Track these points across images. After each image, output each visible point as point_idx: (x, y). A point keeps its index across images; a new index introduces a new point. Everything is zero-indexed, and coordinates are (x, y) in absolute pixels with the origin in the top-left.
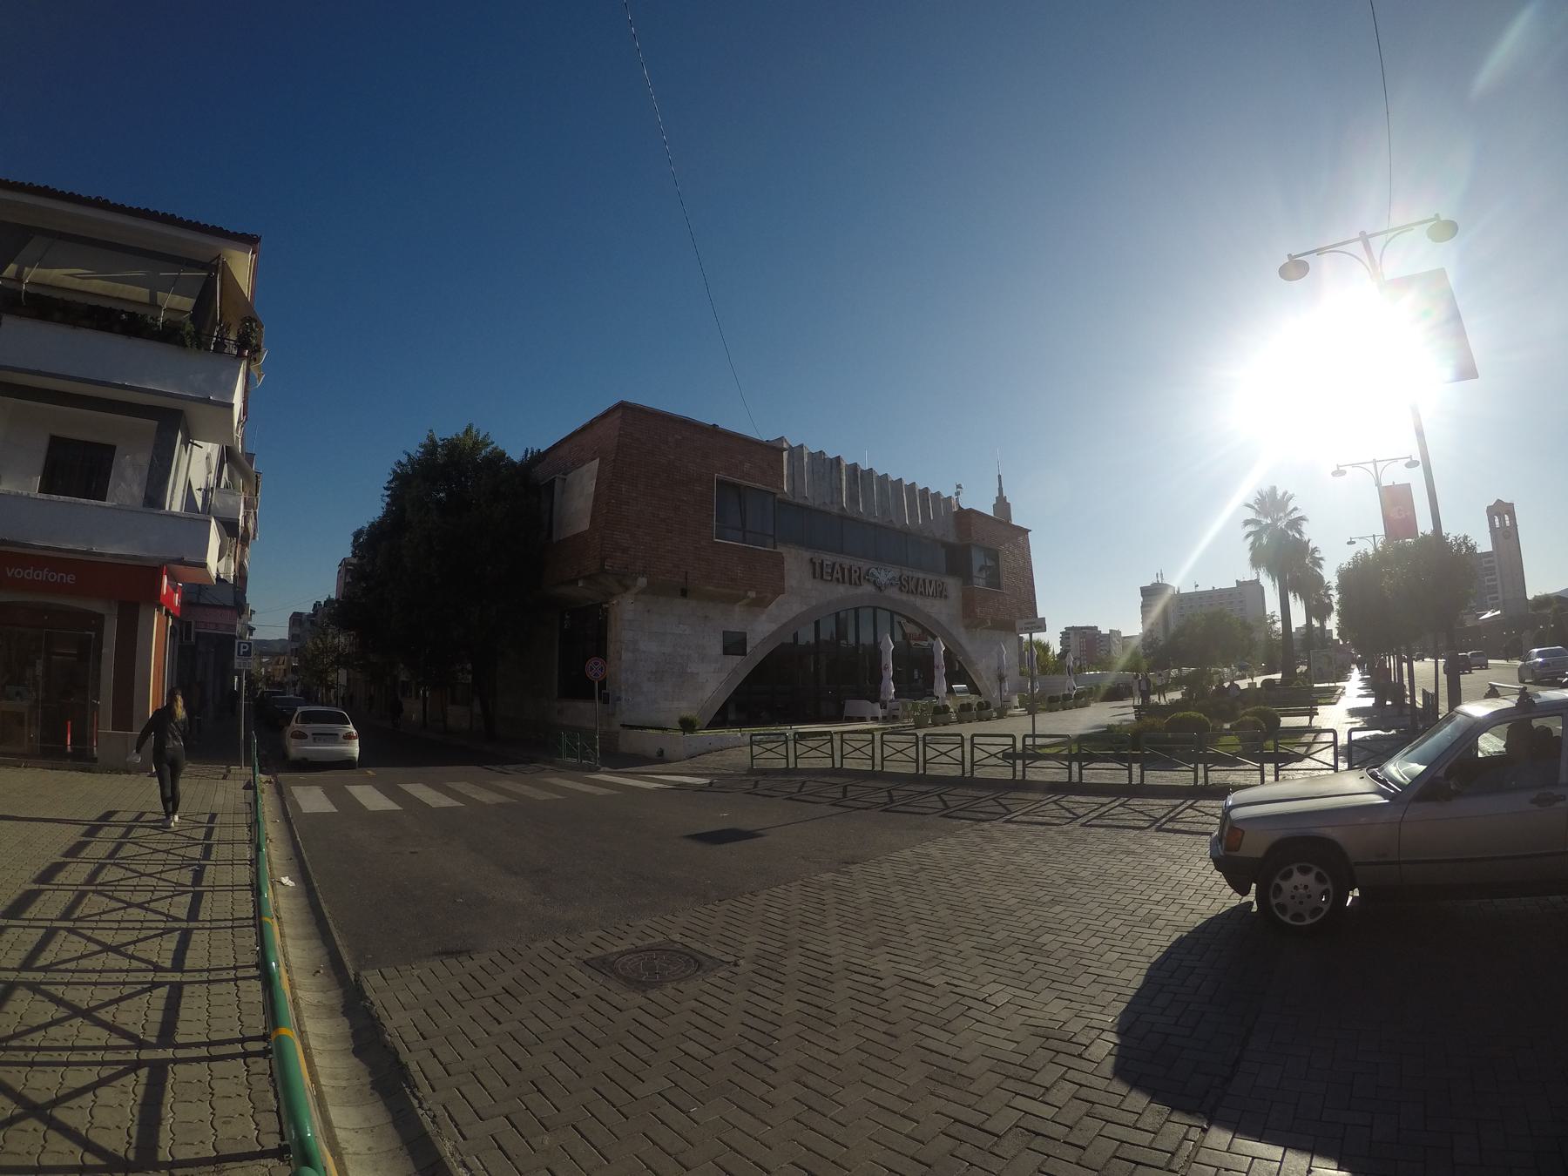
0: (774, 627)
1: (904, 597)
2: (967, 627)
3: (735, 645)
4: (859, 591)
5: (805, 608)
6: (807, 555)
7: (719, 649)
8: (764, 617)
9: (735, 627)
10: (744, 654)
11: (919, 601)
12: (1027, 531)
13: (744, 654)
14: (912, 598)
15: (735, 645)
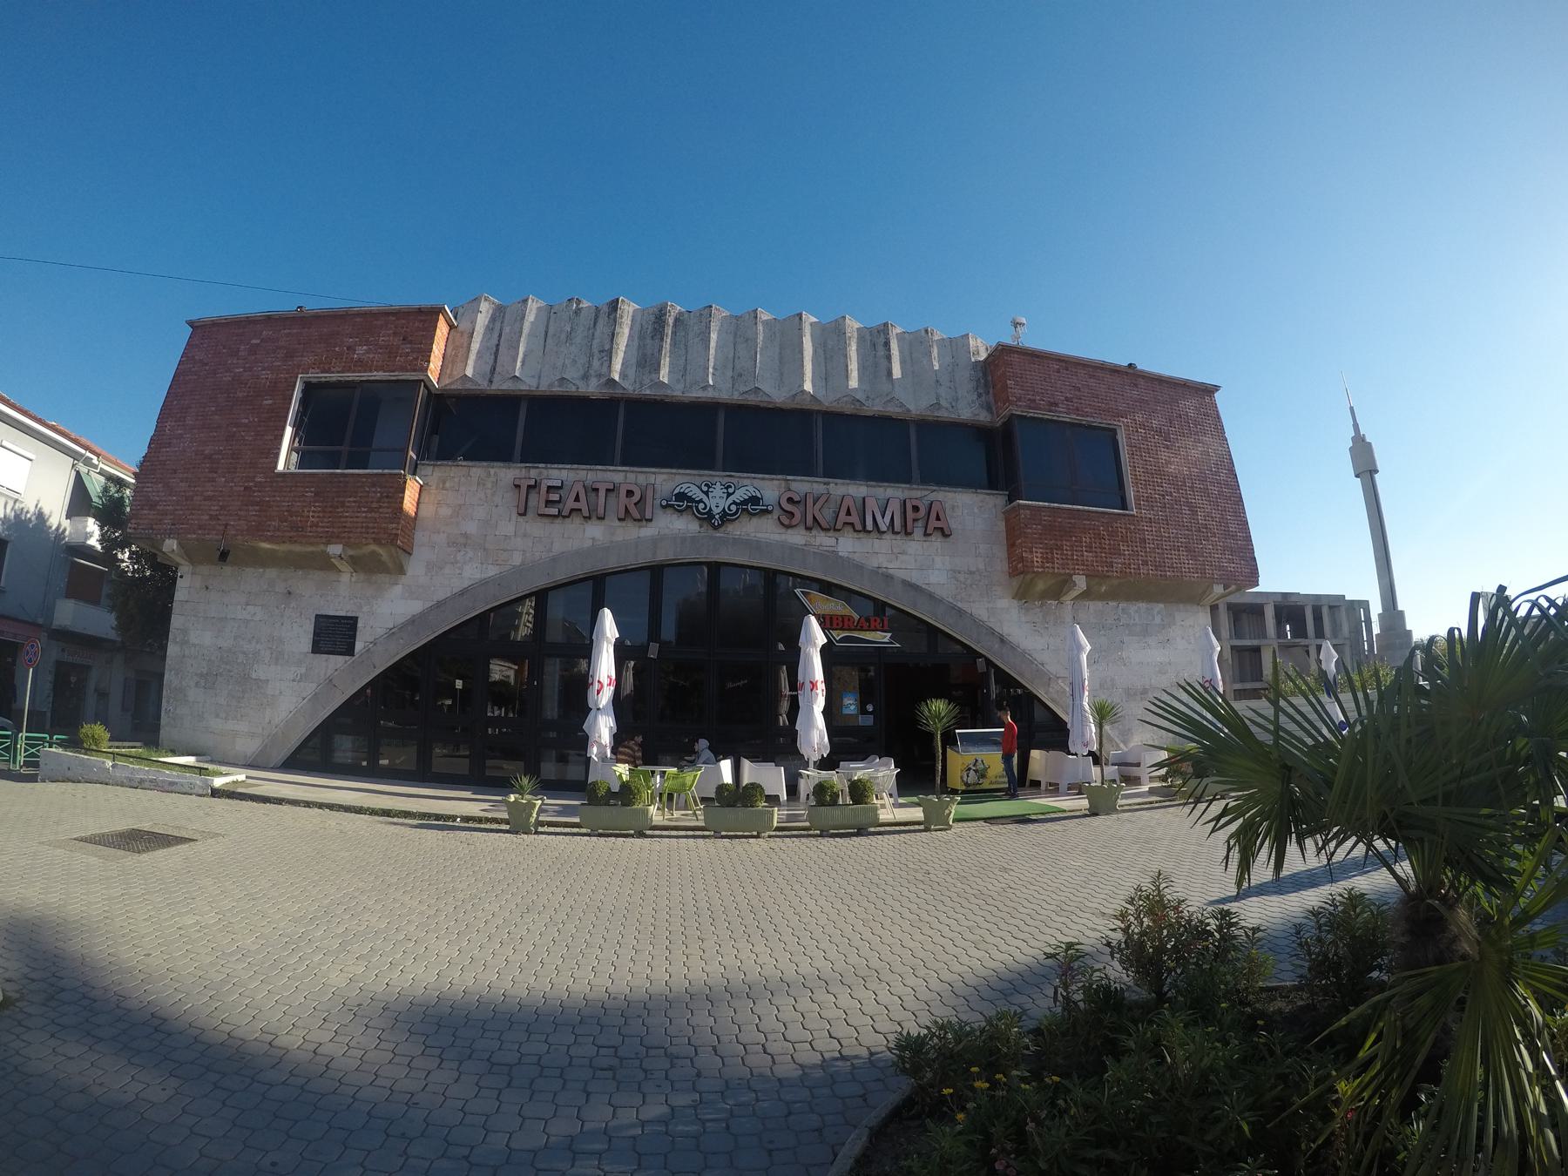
0: (416, 607)
1: (797, 537)
2: (1022, 595)
3: (335, 635)
4: (647, 531)
5: (492, 571)
6: (507, 474)
7: (306, 642)
8: (398, 589)
9: (338, 607)
10: (349, 650)
11: (847, 545)
12: (1209, 391)
13: (349, 650)
14: (824, 540)
15: (335, 635)
